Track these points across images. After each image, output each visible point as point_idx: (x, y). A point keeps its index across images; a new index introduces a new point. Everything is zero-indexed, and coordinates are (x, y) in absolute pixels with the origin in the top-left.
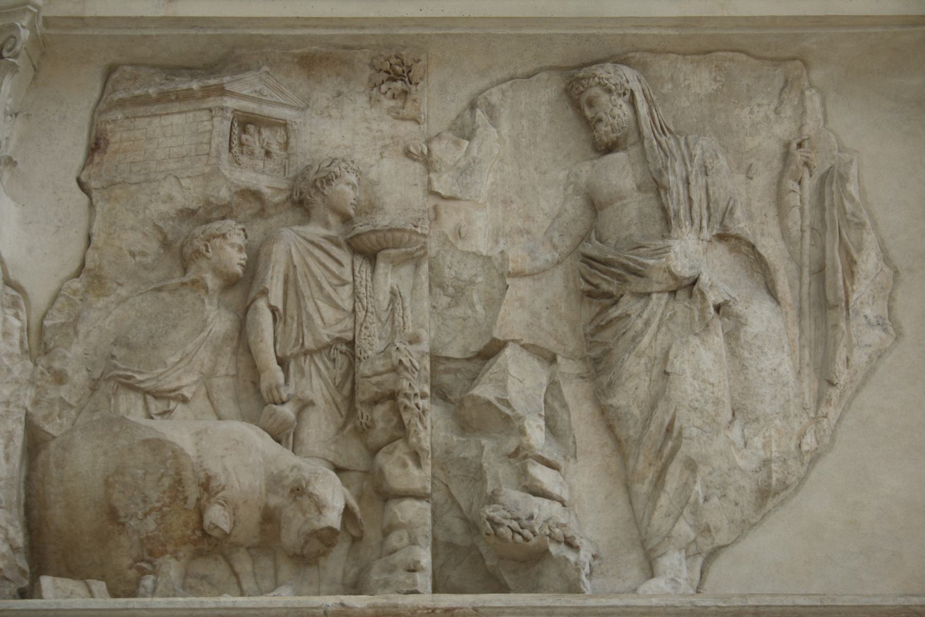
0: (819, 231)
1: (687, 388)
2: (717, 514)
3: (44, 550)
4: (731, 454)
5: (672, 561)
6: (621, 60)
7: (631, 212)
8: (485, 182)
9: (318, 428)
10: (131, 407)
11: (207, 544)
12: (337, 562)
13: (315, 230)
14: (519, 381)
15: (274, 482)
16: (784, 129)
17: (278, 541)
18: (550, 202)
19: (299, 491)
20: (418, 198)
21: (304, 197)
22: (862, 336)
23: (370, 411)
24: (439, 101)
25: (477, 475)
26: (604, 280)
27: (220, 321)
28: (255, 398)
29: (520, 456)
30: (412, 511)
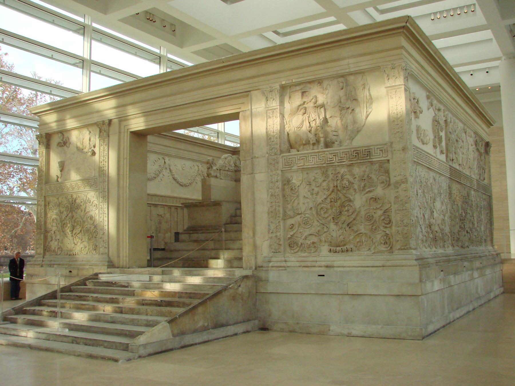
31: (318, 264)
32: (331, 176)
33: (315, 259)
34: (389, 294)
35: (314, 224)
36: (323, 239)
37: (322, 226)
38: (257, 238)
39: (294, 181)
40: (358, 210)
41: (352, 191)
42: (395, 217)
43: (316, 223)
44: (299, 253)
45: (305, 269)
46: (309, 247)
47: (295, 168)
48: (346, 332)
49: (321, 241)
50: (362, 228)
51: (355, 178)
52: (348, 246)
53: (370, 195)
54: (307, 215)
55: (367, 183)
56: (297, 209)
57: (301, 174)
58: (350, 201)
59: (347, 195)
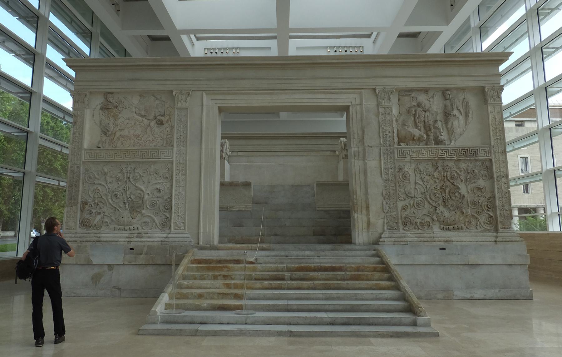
0: (466, 108)
1: (455, 126)
3: (400, 141)
5: (453, 141)
8: (435, 103)
9: (422, 129)
10: (406, 127)
11: (414, 140)
12: (425, 142)
13: (421, 109)
14: (439, 124)
15: (419, 135)
16: (463, 97)
17: (420, 140)
19: (422, 136)
20: (429, 105)
21: (419, 105)
22: (470, 119)
23: (427, 128)
24: (430, 94)
26: (447, 115)
27: (413, 119)
28: (417, 127)
29: (440, 132)
30: (432, 138)
31: (436, 239)
32: (440, 168)
33: (431, 235)
34: (502, 263)
37: (433, 208)
39: (406, 169)
41: (459, 180)
42: (498, 204)
43: (427, 205)
45: (426, 243)
46: (422, 224)
48: (468, 296)
49: (433, 220)
53: (474, 185)
54: (420, 199)
56: (411, 193)
58: (459, 188)
59: (455, 184)
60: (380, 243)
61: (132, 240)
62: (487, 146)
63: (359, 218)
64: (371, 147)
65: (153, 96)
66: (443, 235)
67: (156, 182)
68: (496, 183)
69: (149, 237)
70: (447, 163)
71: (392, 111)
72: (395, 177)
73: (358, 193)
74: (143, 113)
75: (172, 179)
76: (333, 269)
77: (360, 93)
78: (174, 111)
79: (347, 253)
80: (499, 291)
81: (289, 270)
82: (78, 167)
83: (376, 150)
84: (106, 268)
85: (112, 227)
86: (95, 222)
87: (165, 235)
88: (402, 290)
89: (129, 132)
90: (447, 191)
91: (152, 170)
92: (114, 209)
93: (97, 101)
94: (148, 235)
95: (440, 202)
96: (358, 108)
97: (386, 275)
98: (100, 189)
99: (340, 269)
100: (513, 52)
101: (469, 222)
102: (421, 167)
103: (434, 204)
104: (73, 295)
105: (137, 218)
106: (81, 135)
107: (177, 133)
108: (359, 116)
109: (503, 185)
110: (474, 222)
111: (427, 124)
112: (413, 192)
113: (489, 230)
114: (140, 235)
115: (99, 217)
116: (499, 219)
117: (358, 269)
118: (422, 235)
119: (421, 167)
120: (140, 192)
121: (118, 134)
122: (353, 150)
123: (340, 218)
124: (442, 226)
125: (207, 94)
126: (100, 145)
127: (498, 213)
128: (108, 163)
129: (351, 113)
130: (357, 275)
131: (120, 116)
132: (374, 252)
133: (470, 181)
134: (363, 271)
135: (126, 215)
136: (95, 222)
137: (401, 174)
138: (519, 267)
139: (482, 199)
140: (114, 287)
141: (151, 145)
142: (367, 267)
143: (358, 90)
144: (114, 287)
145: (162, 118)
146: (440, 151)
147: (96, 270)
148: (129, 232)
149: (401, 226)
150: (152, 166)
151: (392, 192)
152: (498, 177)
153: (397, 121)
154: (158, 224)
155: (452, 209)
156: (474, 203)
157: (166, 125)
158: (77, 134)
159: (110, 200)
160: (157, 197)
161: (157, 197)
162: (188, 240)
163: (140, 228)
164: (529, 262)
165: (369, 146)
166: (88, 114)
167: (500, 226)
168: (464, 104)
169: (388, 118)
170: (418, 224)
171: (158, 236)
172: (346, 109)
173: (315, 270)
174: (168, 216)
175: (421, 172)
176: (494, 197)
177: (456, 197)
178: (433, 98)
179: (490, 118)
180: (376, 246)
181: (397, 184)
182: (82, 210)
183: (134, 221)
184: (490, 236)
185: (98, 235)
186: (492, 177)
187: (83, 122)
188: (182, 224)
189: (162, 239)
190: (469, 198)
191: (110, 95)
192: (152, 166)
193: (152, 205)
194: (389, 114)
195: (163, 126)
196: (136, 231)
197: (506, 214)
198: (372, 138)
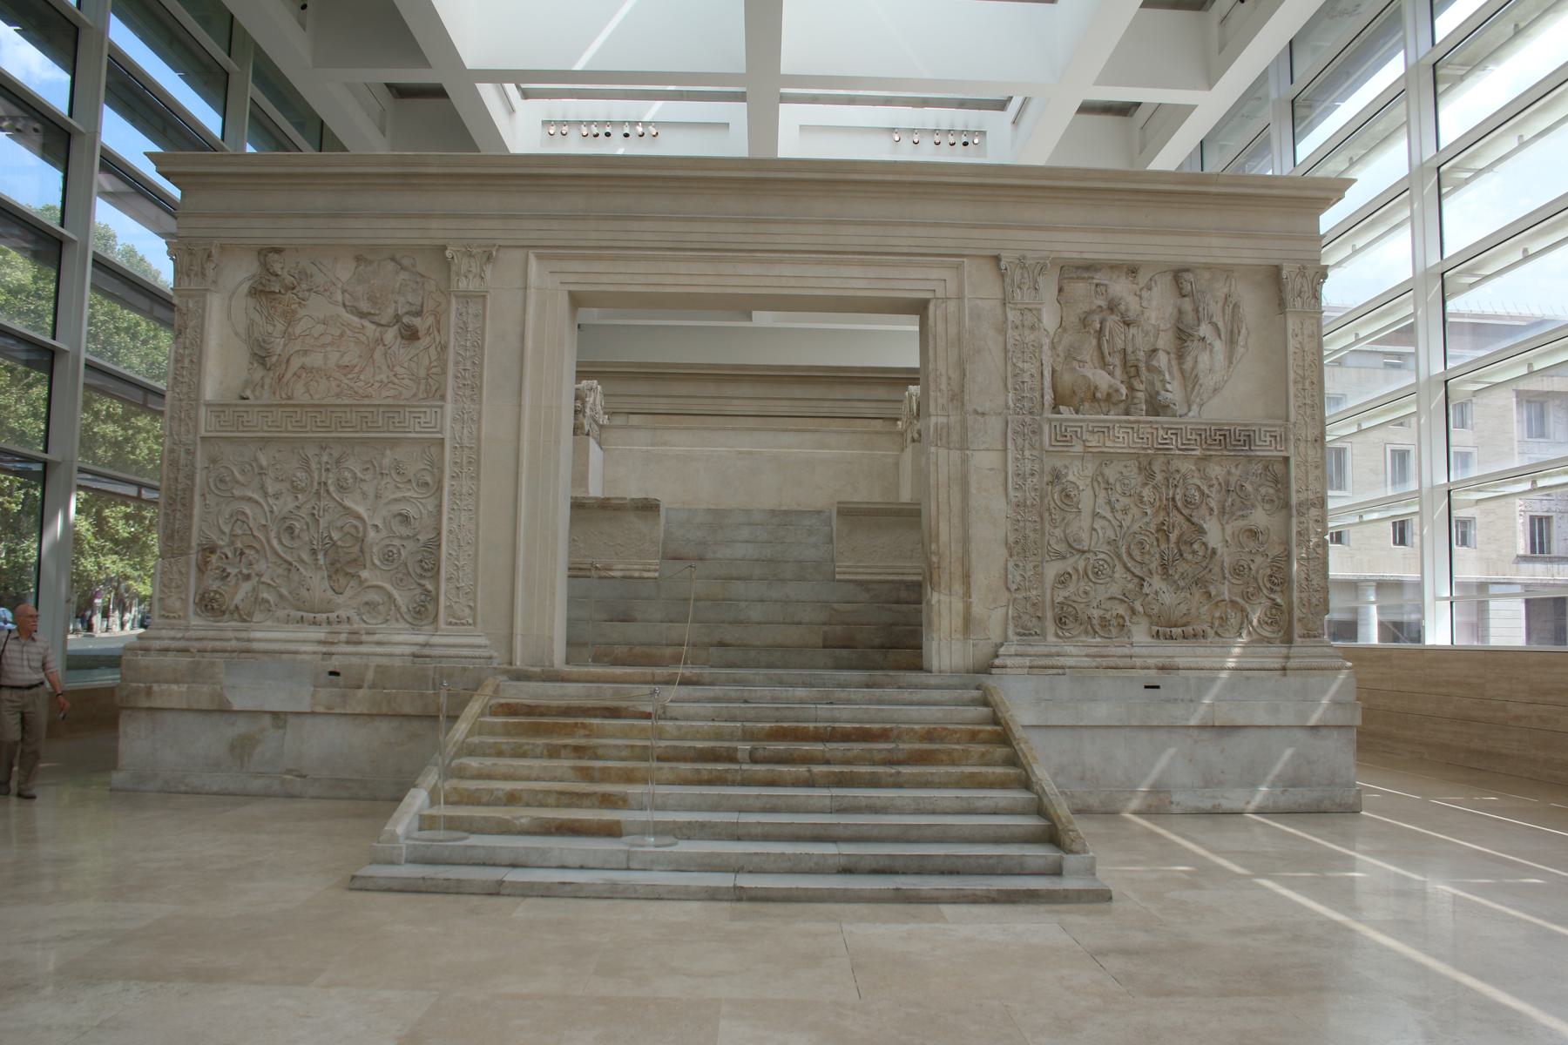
1: (1201, 366)
2: (1205, 396)
4: (1208, 382)
5: (1195, 407)
6: (1187, 270)
7: (1190, 317)
8: (1154, 303)
9: (1118, 372)
10: (1075, 364)
11: (1094, 398)
12: (1122, 406)
13: (1115, 318)
14: (1162, 360)
16: (1226, 290)
18: (1170, 310)
19: (1117, 391)
21: (1112, 307)
22: (1240, 350)
23: (1131, 371)
24: (1143, 279)
25: (1153, 384)
26: (1183, 335)
27: (1094, 342)
28: (1104, 364)
29: (1163, 381)
30: (1141, 395)
31: (1138, 662)
32: (1159, 477)
33: (1126, 651)
35: (1117, 576)
36: (1141, 609)
37: (1136, 580)
38: (974, 599)
39: (1071, 477)
40: (1219, 552)
41: (1204, 510)
44: (1083, 638)
45: (1111, 672)
47: (1078, 448)
48: (1207, 804)
49: (1134, 612)
50: (1225, 591)
51: (1211, 486)
52: (1199, 628)
53: (1241, 523)
54: (1101, 556)
55: (1235, 500)
56: (1080, 541)
57: (1089, 465)
59: (1195, 519)
60: (994, 671)
61: (334, 649)
62: (1280, 422)
63: (943, 607)
64: (983, 414)
65: (393, 259)
66: (1155, 651)
67: (399, 495)
68: (1294, 520)
69: (379, 643)
70: (1176, 464)
71: (1039, 320)
72: (1042, 498)
73: (944, 537)
74: (364, 306)
75: (440, 488)
76: (865, 736)
77: (959, 267)
78: (449, 302)
79: (905, 695)
80: (1283, 792)
81: (748, 736)
82: (188, 452)
83: (995, 424)
84: (267, 720)
85: (281, 613)
86: (238, 599)
87: (421, 639)
88: (1037, 788)
89: (326, 358)
90: (1173, 537)
91: (386, 462)
92: (285, 566)
93: (239, 273)
94: (377, 637)
95: (1154, 565)
96: (952, 306)
97: (1000, 752)
98: (248, 511)
99: (883, 735)
100: (1354, 181)
101: (1224, 620)
102: (1111, 473)
103: (1137, 571)
104: (183, 788)
105: (349, 593)
106: (198, 362)
107: (457, 363)
108: (953, 330)
109: (1312, 525)
110: (1234, 620)
111: (1131, 358)
112: (1085, 536)
113: (1269, 641)
114: (354, 638)
115: (246, 587)
116: (1297, 613)
117: (929, 736)
118: (1104, 651)
119: (1111, 473)
120: (355, 522)
121: (296, 363)
122: (933, 420)
123: (897, 602)
124: (1155, 628)
125: (539, 257)
126: (248, 393)
127: (1295, 595)
128: (268, 440)
129: (931, 322)
130: (926, 752)
131: (302, 312)
132: (976, 694)
133: (1233, 513)
134: (942, 740)
135: (317, 584)
136: (238, 599)
137: (1057, 488)
138: (1335, 733)
139: (1259, 560)
140: (289, 772)
141: (384, 394)
142: (955, 732)
143: (954, 257)
144: (289, 772)
145: (417, 321)
146: (1161, 432)
147: (242, 727)
148: (325, 629)
149: (1051, 627)
150: (388, 452)
151: (1032, 536)
152: (1300, 504)
153: (1053, 347)
154: (404, 609)
155: (1182, 583)
156: (1237, 571)
157: (424, 341)
158: (187, 361)
159: (275, 543)
160: (401, 537)
161: (401, 537)
162: (485, 653)
163: (355, 618)
164: (1358, 722)
165: (976, 412)
166: (215, 305)
167: (1298, 629)
168: (1229, 310)
169: (1030, 337)
170: (1095, 622)
171: (399, 640)
172: (919, 308)
173: (818, 737)
174: (429, 587)
175: (1109, 487)
176: (1288, 557)
177: (1194, 552)
178: (1150, 289)
179: (1291, 349)
180: (983, 678)
181: (1046, 515)
182: (202, 568)
183: (340, 599)
184: (1272, 656)
185: (244, 635)
186: (1286, 505)
187: (202, 329)
188: (467, 611)
189: (415, 649)
190: (1226, 556)
191: (276, 256)
192: (388, 452)
193: (388, 557)
194: (1033, 328)
195: (417, 343)
196: (345, 627)
197: (1314, 600)
198: (987, 391)
